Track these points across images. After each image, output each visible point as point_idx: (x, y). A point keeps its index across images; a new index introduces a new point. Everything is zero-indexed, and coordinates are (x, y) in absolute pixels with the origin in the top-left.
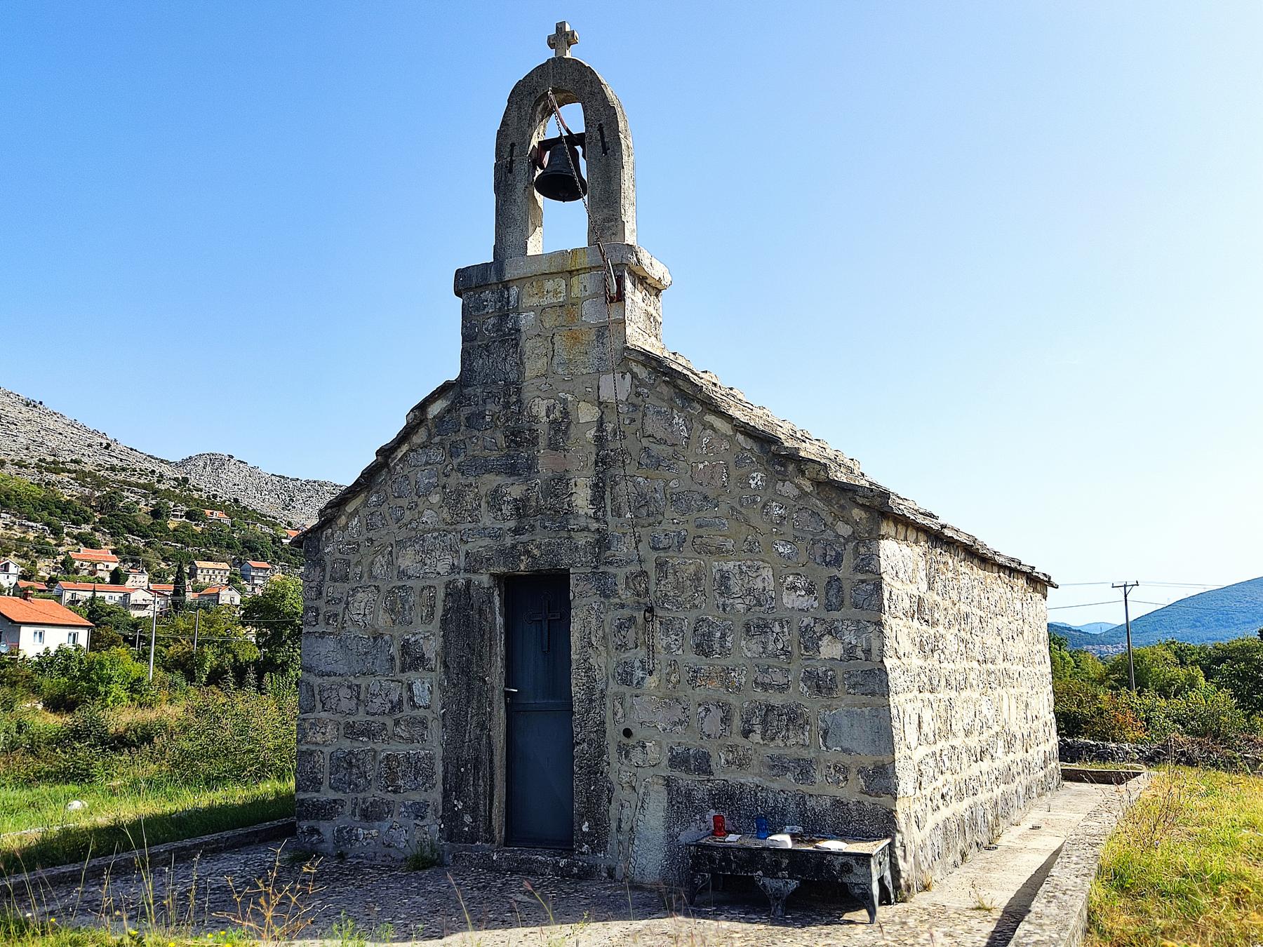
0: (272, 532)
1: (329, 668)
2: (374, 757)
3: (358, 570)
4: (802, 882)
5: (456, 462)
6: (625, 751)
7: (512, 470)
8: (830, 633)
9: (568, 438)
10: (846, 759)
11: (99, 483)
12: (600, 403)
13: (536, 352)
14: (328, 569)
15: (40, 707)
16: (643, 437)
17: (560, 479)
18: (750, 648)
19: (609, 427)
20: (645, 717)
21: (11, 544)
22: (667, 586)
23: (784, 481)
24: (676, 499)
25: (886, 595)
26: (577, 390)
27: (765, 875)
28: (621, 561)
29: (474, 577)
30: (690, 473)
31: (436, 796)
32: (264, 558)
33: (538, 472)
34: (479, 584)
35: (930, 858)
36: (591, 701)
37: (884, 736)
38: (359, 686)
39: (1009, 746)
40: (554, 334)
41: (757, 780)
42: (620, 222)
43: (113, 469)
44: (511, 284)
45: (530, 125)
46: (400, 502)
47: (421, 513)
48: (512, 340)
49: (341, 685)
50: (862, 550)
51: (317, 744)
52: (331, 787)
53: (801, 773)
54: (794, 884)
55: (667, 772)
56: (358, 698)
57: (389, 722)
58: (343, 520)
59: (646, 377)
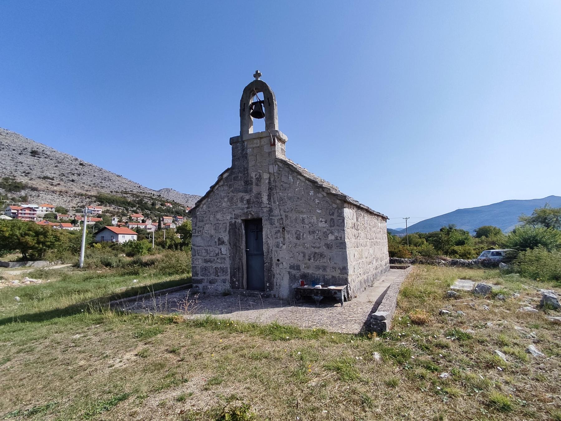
0: (183, 209)
1: (199, 245)
2: (212, 268)
3: (206, 219)
4: (324, 297)
5: (231, 190)
6: (277, 265)
7: (246, 192)
8: (331, 233)
10: (335, 266)
11: (138, 197)
12: (269, 173)
14: (198, 219)
15: (125, 255)
17: (259, 194)
18: (310, 238)
19: (272, 179)
21: (115, 213)
22: (288, 222)
23: (319, 193)
24: (290, 198)
25: (346, 223)
27: (314, 295)
29: (237, 221)
31: (228, 277)
32: (181, 216)
35: (357, 290)
36: (268, 252)
37: (344, 259)
38: (207, 249)
39: (377, 260)
41: (312, 272)
43: (141, 193)
45: (249, 98)
46: (216, 201)
47: (222, 204)
49: (202, 249)
50: (339, 211)
51: (197, 264)
52: (201, 275)
53: (324, 269)
54: (322, 298)
55: (289, 270)
56: (207, 252)
57: (216, 259)
58: (201, 206)
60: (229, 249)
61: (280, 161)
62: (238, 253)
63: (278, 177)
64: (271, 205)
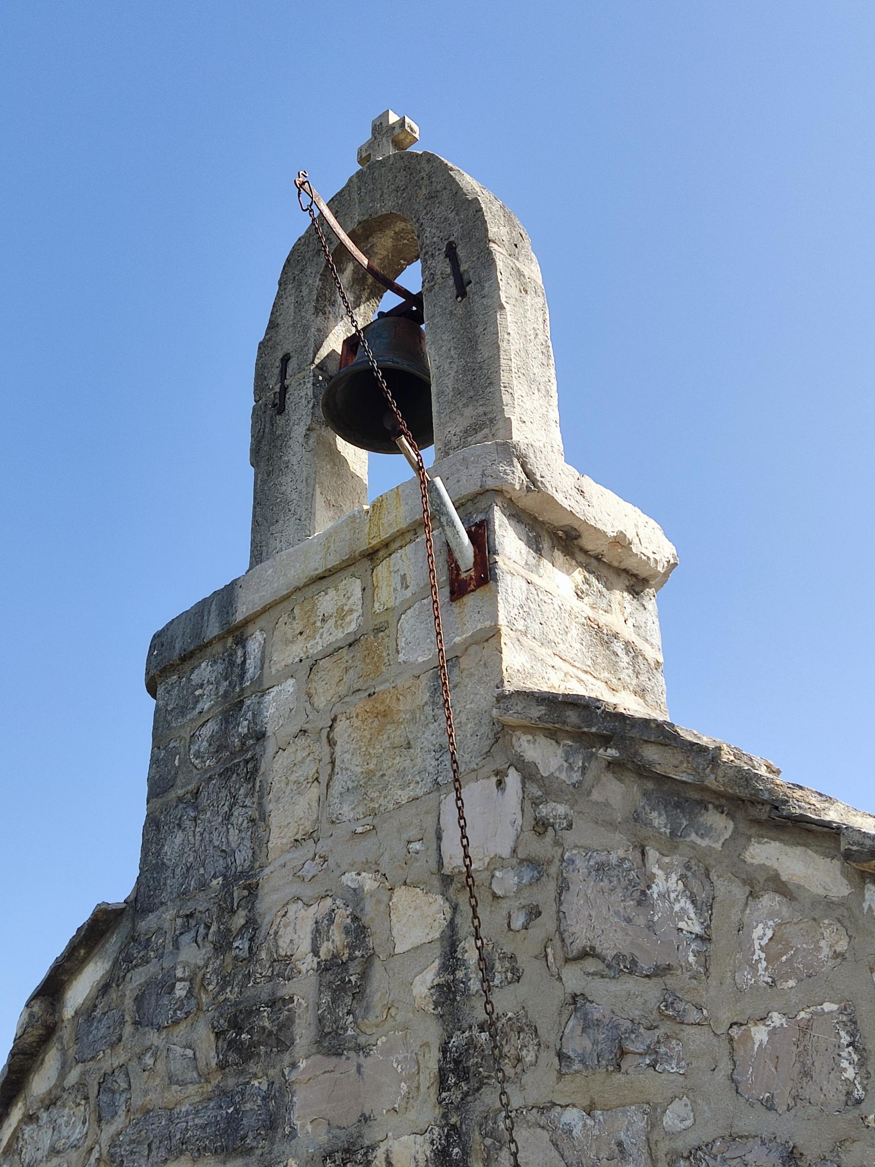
5: (109, 1130)
9: (367, 1009)
12: (447, 880)
13: (293, 778)
16: (567, 960)
26: (386, 857)
30: (725, 1066)
33: (293, 1135)
40: (334, 720)
42: (501, 424)
44: (250, 629)
45: (319, 310)
48: (247, 762)
59: (560, 768)
61: (537, 711)
63: (534, 913)
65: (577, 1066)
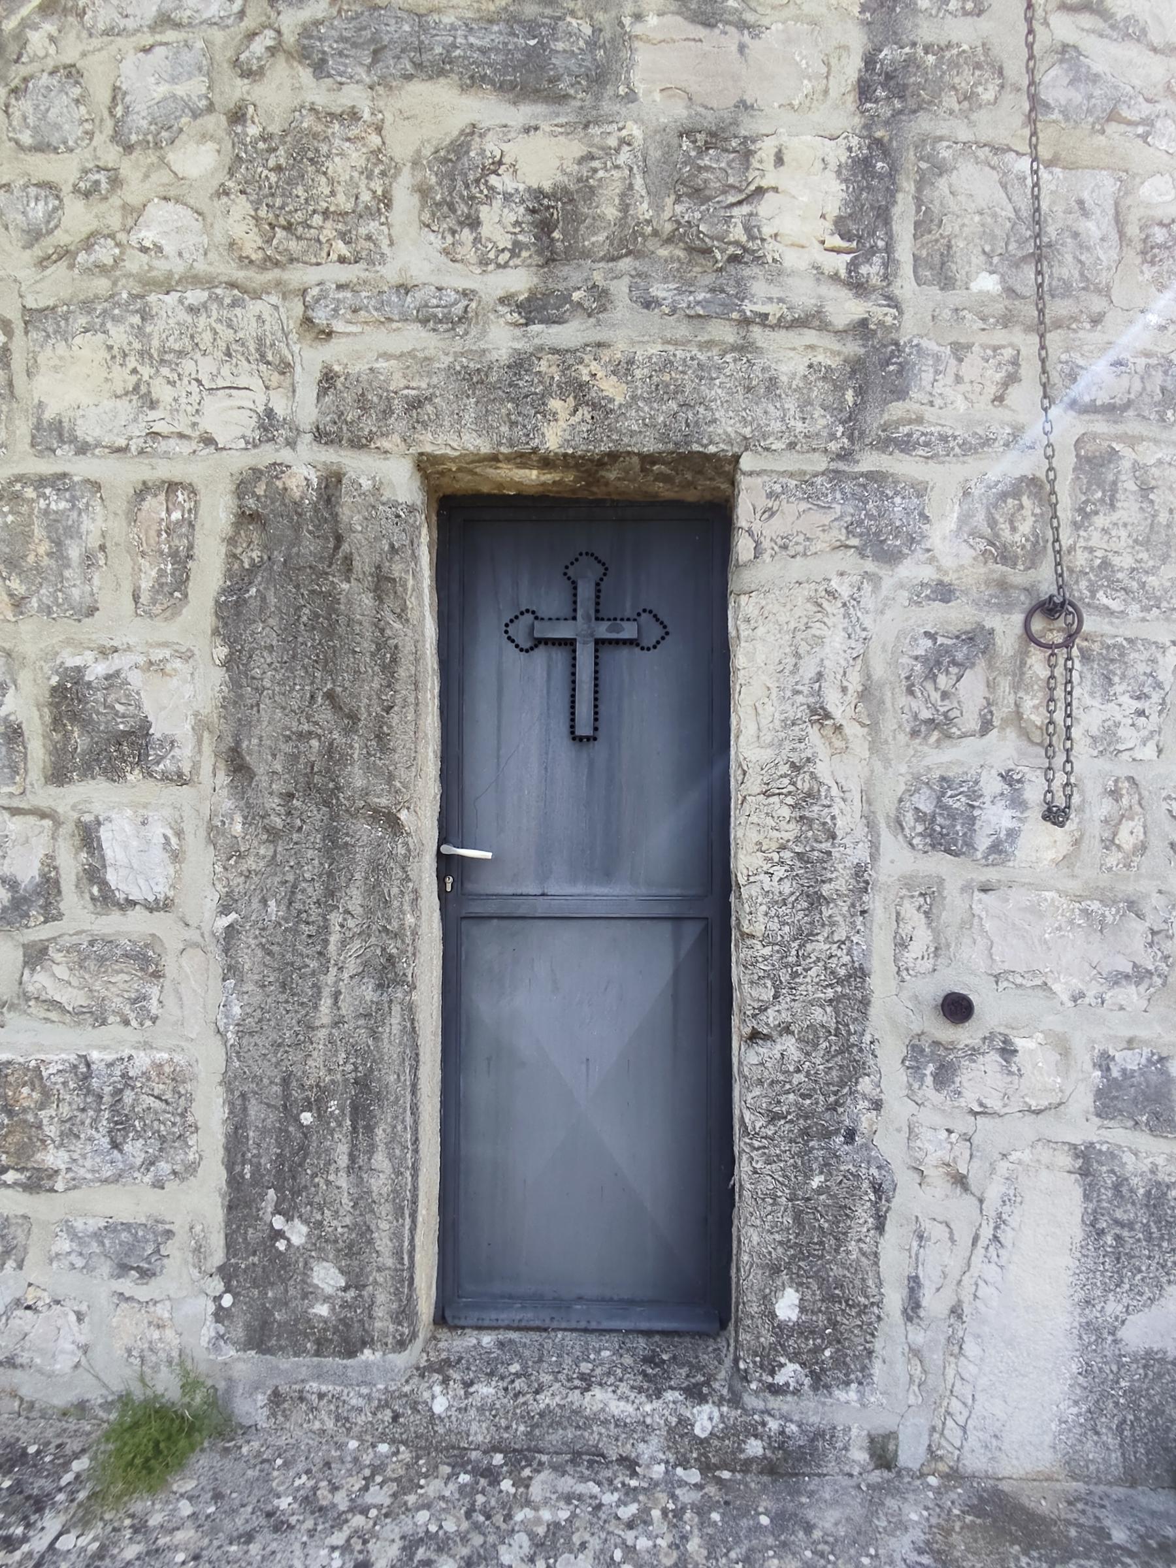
20: (1010, 955)
28: (944, 438)
33: (631, 97)
34: (377, 489)
36: (816, 901)
47: (134, 213)
55: (1088, 1131)
60: (214, 831)
62: (355, 898)
64: (893, 302)
65: (1056, 115)
